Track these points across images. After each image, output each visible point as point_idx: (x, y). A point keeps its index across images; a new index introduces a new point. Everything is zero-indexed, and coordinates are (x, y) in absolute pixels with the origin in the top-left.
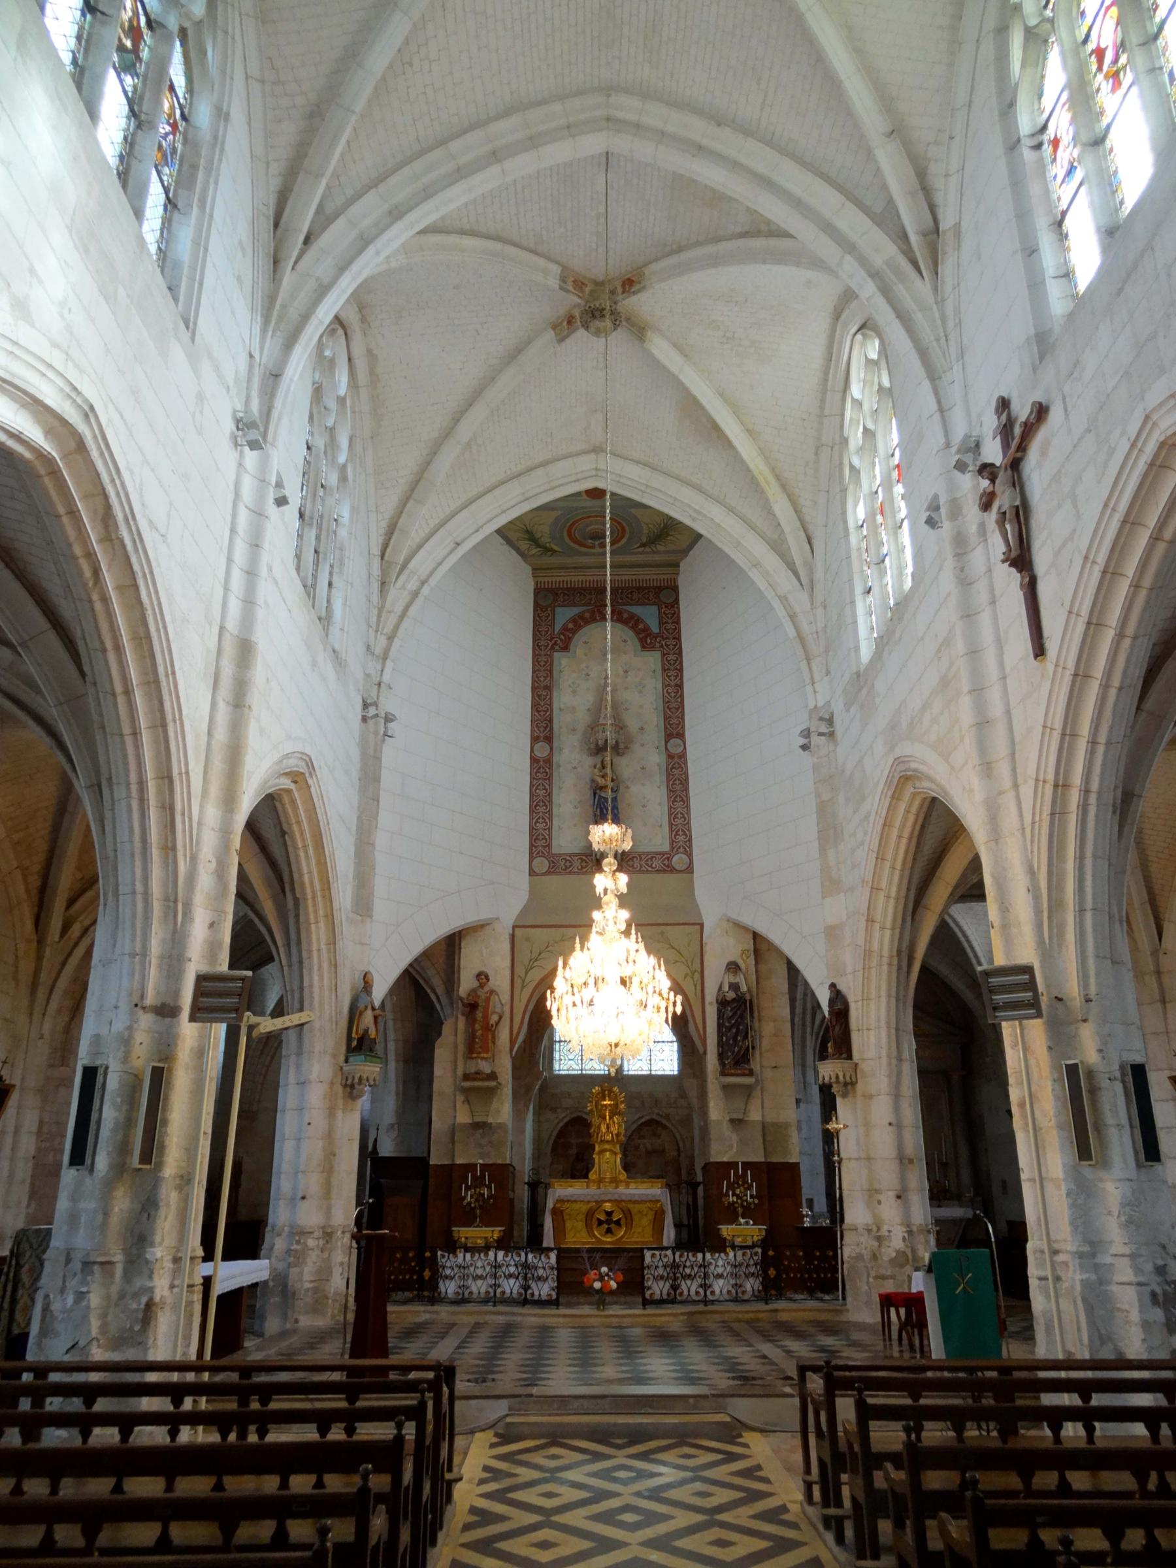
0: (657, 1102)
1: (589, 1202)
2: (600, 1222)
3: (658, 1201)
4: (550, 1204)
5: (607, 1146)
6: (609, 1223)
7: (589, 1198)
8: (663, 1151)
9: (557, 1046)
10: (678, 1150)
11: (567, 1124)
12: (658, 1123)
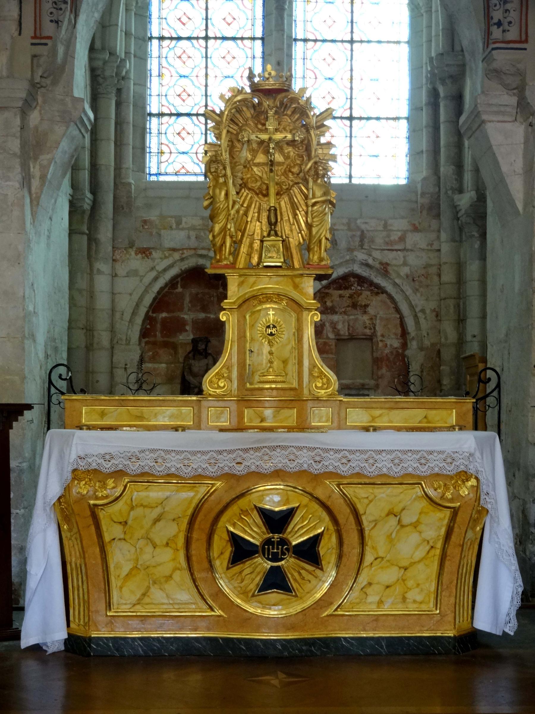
0: (363, 240)
1: (199, 478)
2: (241, 551)
3: (464, 476)
4: (50, 486)
5: (267, 283)
6: (277, 551)
7: (199, 464)
8: (370, 338)
9: (154, 124)
10: (404, 333)
11: (172, 283)
12: (361, 280)
